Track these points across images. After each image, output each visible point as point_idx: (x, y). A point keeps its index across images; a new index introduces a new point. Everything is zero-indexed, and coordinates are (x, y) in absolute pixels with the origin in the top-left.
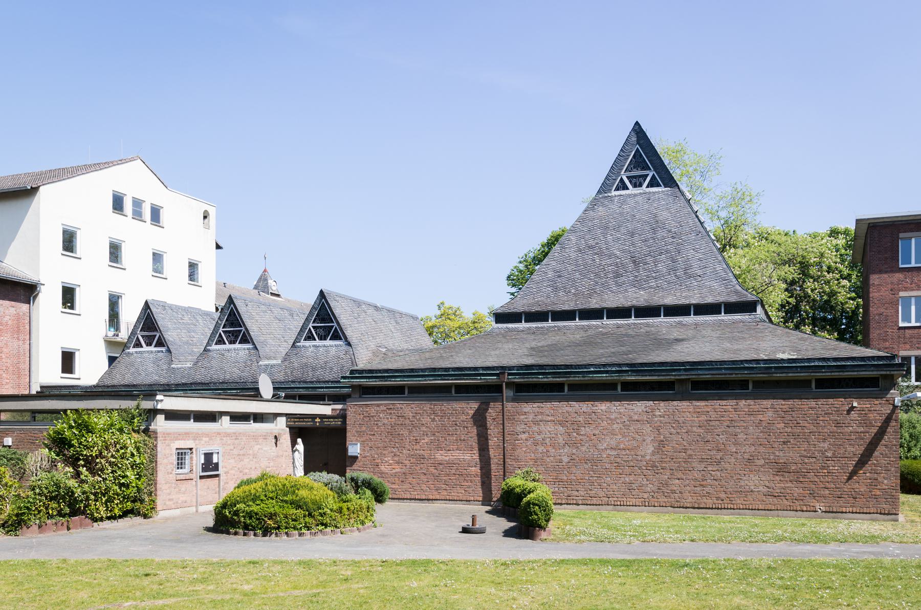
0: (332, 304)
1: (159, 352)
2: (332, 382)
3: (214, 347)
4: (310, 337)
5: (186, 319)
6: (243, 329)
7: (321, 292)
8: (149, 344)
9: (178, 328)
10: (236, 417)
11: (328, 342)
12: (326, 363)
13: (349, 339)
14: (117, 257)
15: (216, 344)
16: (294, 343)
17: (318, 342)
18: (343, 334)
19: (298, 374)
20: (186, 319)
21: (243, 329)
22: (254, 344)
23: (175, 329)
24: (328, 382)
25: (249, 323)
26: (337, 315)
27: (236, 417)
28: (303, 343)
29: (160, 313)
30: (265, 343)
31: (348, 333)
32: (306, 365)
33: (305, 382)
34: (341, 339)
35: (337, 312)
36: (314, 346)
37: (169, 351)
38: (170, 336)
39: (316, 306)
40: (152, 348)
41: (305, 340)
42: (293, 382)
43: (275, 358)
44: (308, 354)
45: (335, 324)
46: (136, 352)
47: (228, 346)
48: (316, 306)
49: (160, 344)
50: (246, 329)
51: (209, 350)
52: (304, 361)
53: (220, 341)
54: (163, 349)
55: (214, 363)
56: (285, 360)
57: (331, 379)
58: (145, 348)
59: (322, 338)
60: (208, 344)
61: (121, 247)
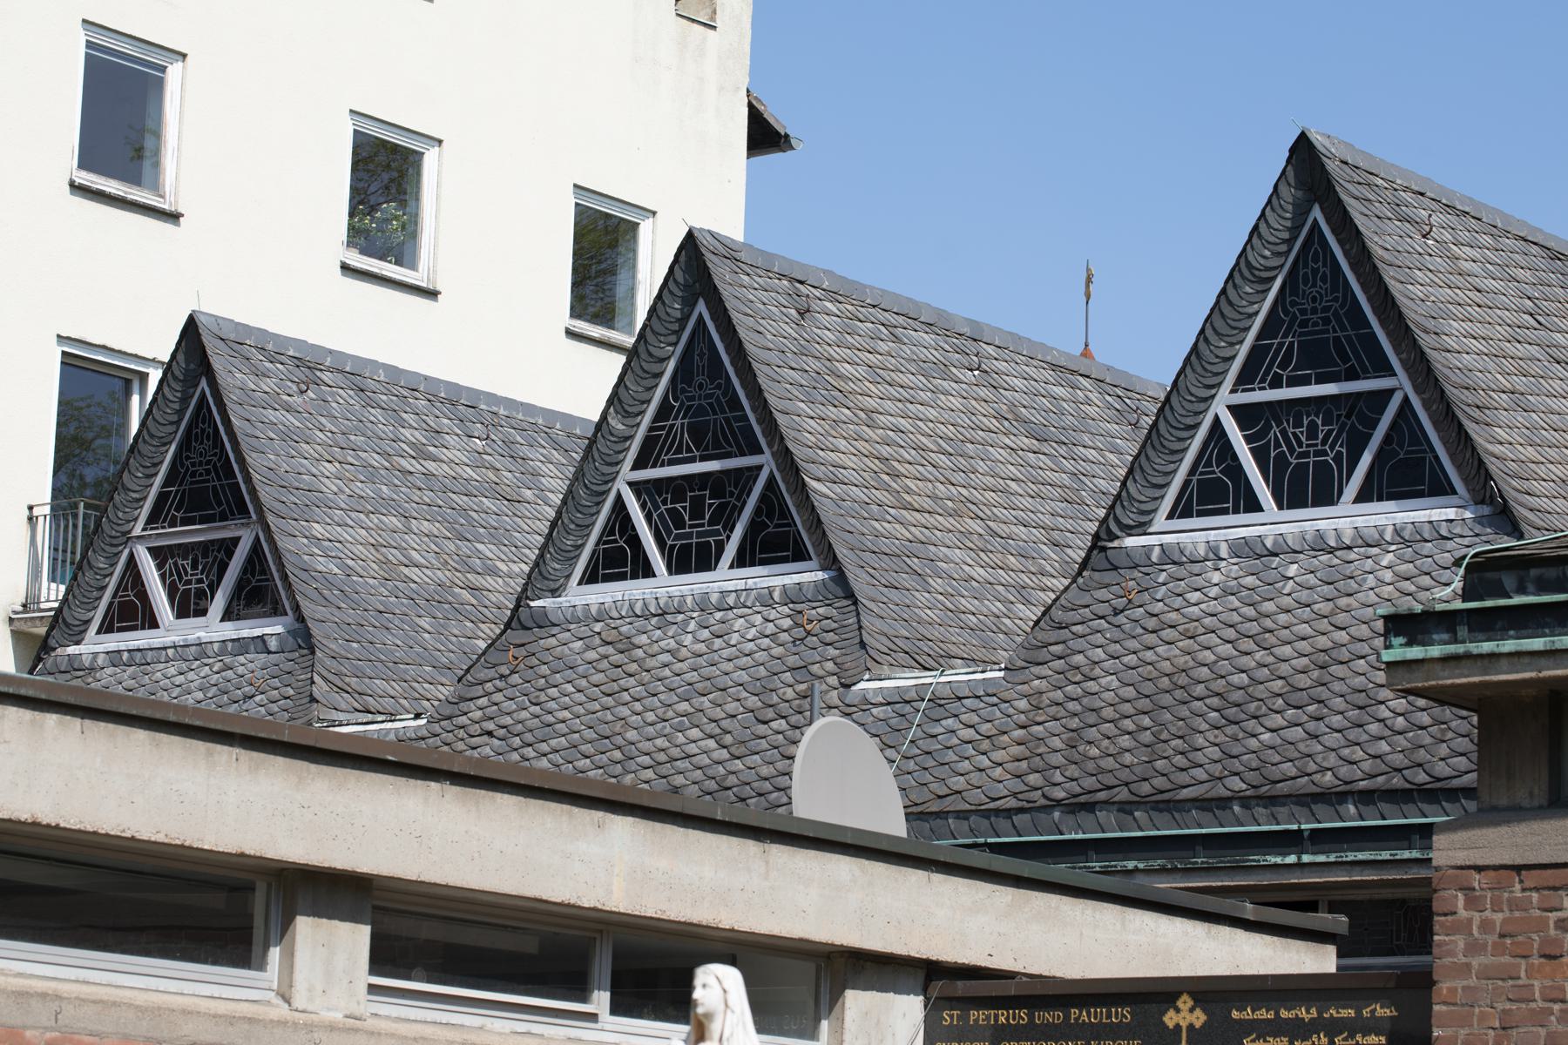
0: (1382, 238)
1: (242, 646)
2: (1367, 798)
3: (580, 596)
4: (1217, 490)
5: (455, 453)
6: (766, 461)
7: (1304, 152)
8: (189, 605)
9: (384, 506)
10: (431, 939)
11: (1346, 517)
12: (1324, 661)
13: (1510, 487)
14: (139, 153)
15: (591, 577)
16: (1098, 543)
17: (1273, 522)
18: (1461, 442)
19: (1117, 753)
20: (455, 453)
21: (766, 461)
22: (831, 561)
23: (358, 504)
24: (1332, 798)
25: (803, 424)
26: (1413, 313)
27: (431, 939)
28: (1165, 533)
29: (273, 401)
30: (912, 560)
31: (1502, 441)
32: (1180, 684)
33: (1165, 805)
34: (1439, 488)
35: (1416, 293)
36: (1245, 550)
37: (303, 639)
38: (325, 541)
39: (1262, 257)
40: (212, 628)
41: (1182, 509)
42: (1079, 807)
43: (986, 664)
44: (1197, 605)
45: (1401, 382)
46: (114, 657)
47: (664, 585)
48: (1262, 257)
49: (259, 591)
50: (786, 458)
51: (543, 622)
52: (1169, 655)
53: (619, 559)
54: (273, 628)
55: (567, 702)
56: (1031, 655)
57: (1359, 774)
58: (172, 630)
59: (1305, 487)
60: (541, 578)
61: (159, 84)
